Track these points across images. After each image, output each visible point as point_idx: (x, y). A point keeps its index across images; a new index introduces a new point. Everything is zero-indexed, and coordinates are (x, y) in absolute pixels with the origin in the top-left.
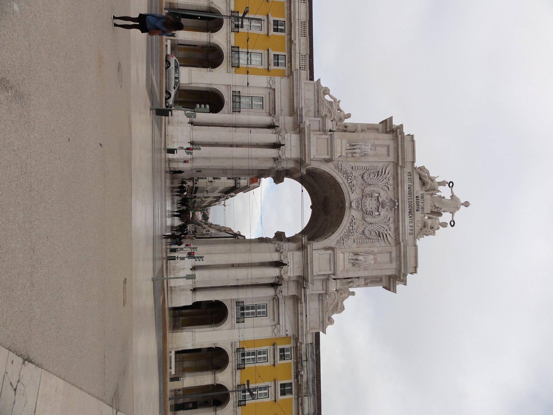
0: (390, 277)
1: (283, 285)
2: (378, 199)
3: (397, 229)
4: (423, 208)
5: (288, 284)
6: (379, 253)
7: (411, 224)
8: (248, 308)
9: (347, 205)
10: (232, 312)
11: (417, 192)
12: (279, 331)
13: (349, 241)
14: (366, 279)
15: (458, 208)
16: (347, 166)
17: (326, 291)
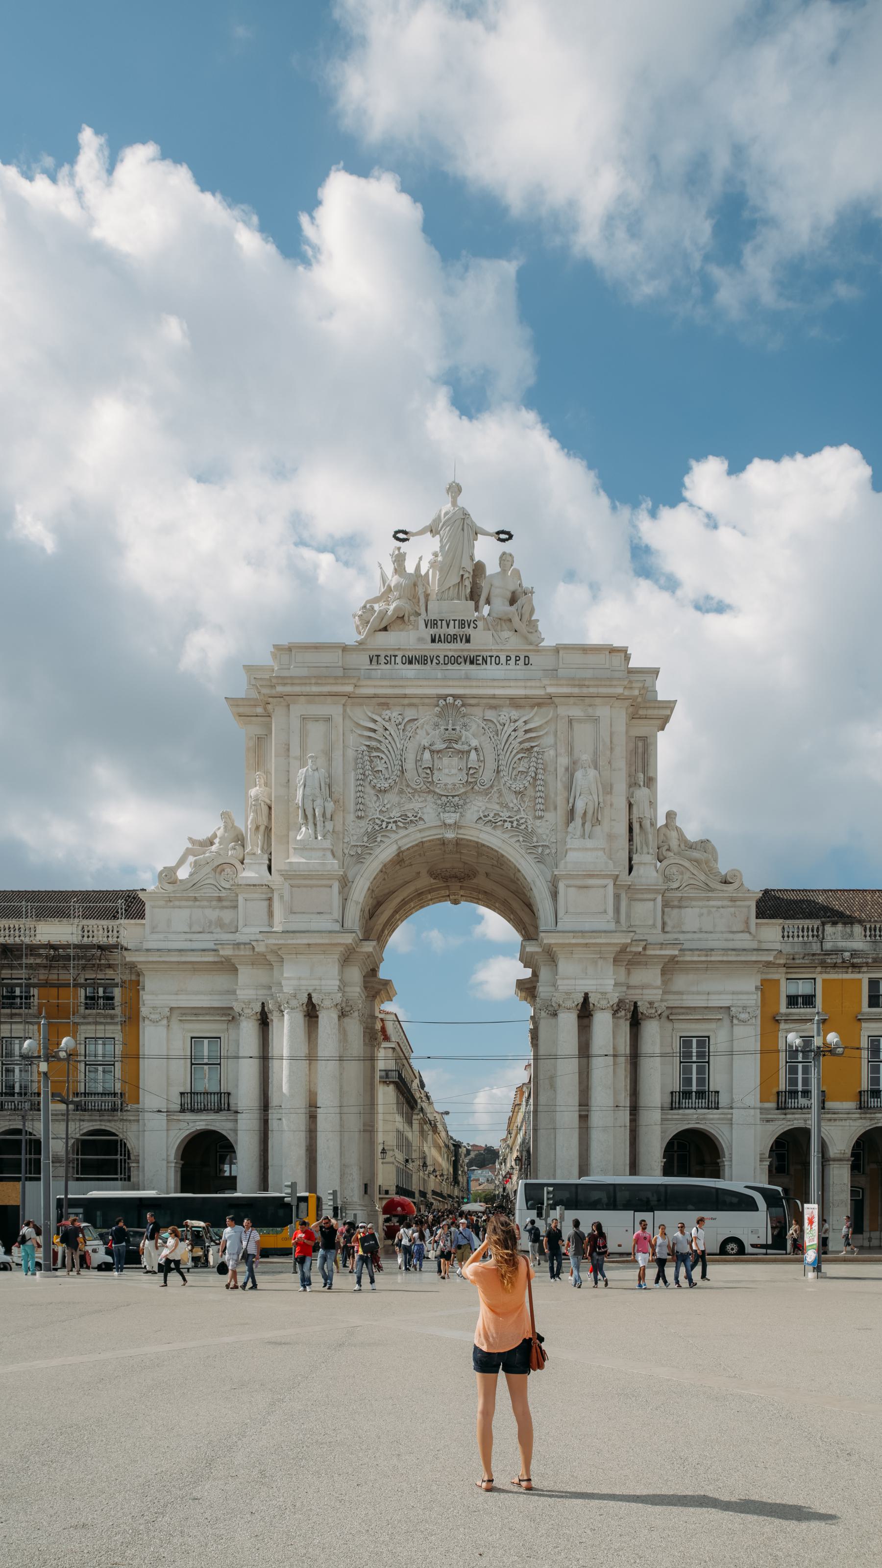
0: (634, 717)
1: (635, 998)
2: (438, 752)
3: (515, 702)
4: (462, 624)
5: (635, 987)
6: (571, 751)
7: (503, 660)
8: (688, 1081)
9: (450, 835)
10: (692, 1118)
11: (420, 640)
12: (744, 1008)
13: (540, 831)
14: (633, 784)
15: (465, 516)
16: (356, 830)
17: (656, 891)
